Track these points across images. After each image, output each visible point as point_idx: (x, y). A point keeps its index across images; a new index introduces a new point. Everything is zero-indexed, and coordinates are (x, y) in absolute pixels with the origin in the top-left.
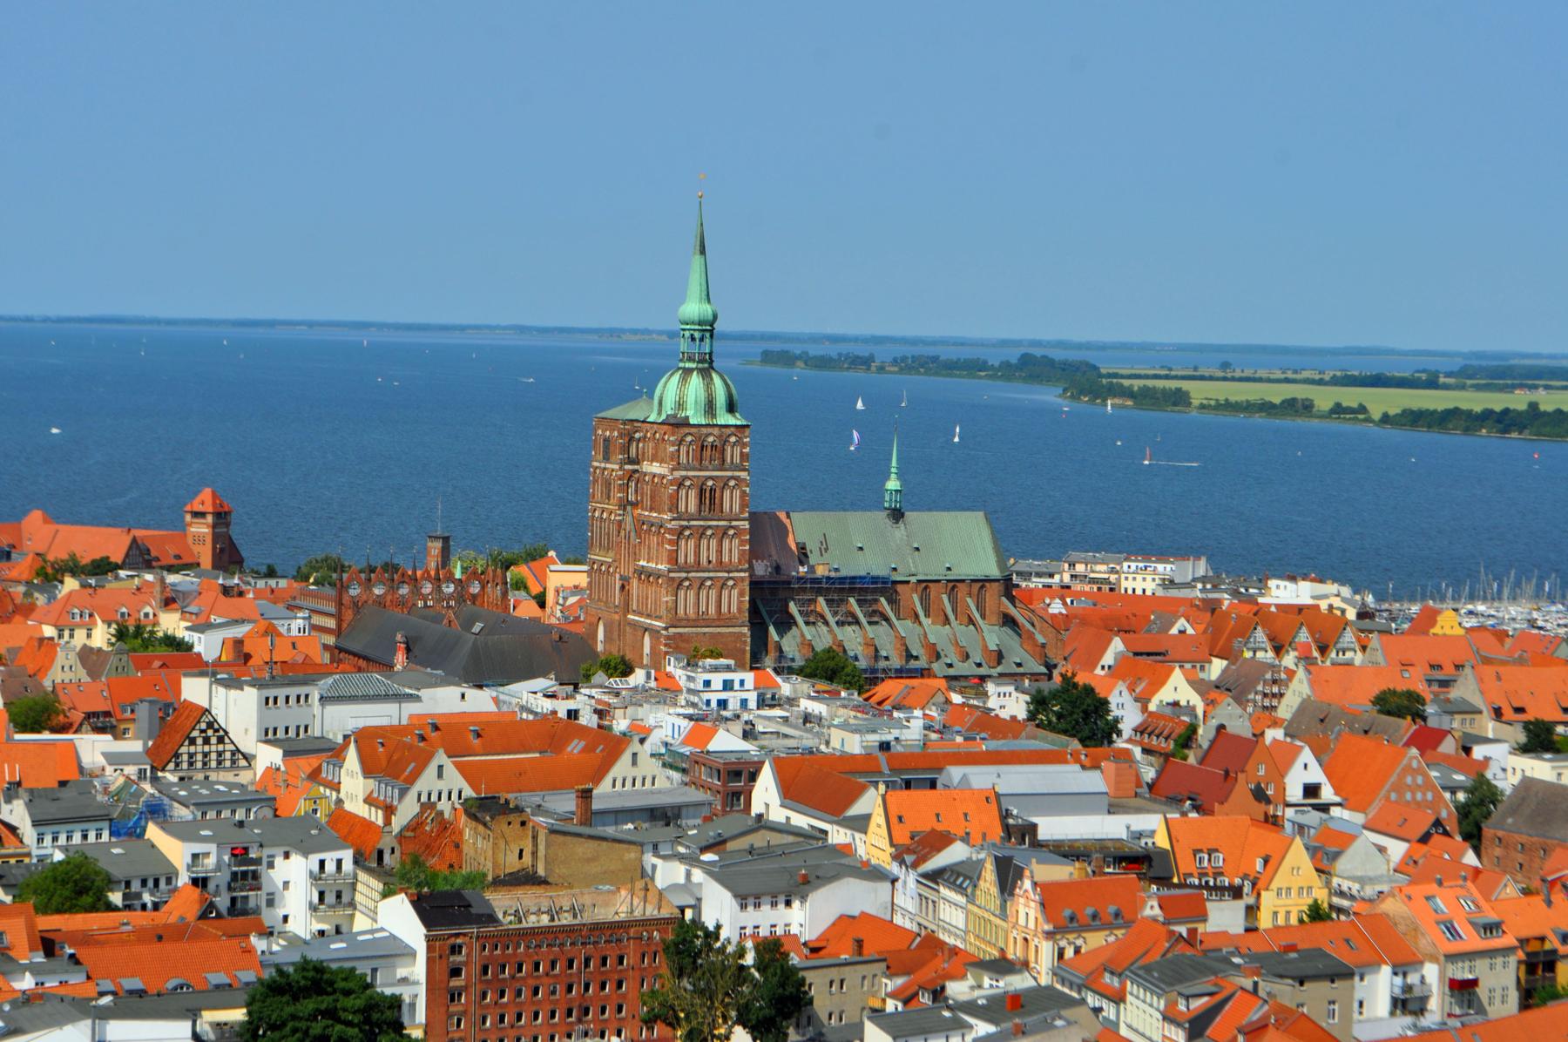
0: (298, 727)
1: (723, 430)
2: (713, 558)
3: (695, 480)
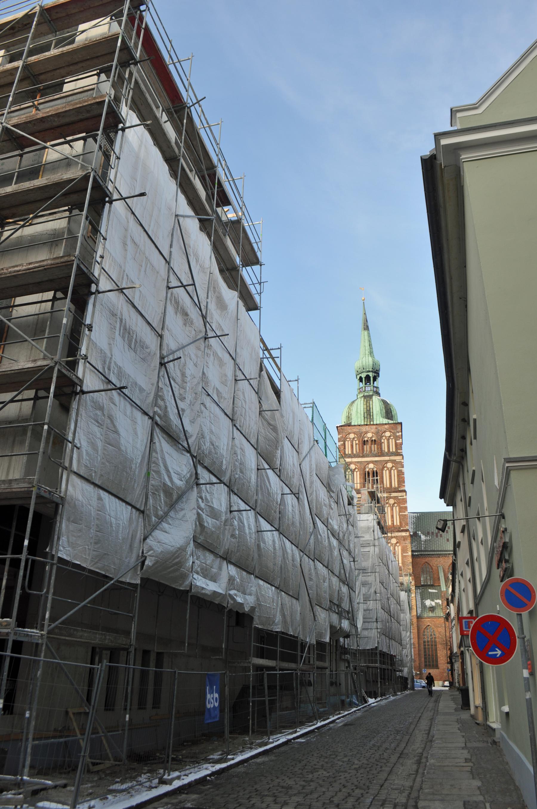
3: (359, 465)
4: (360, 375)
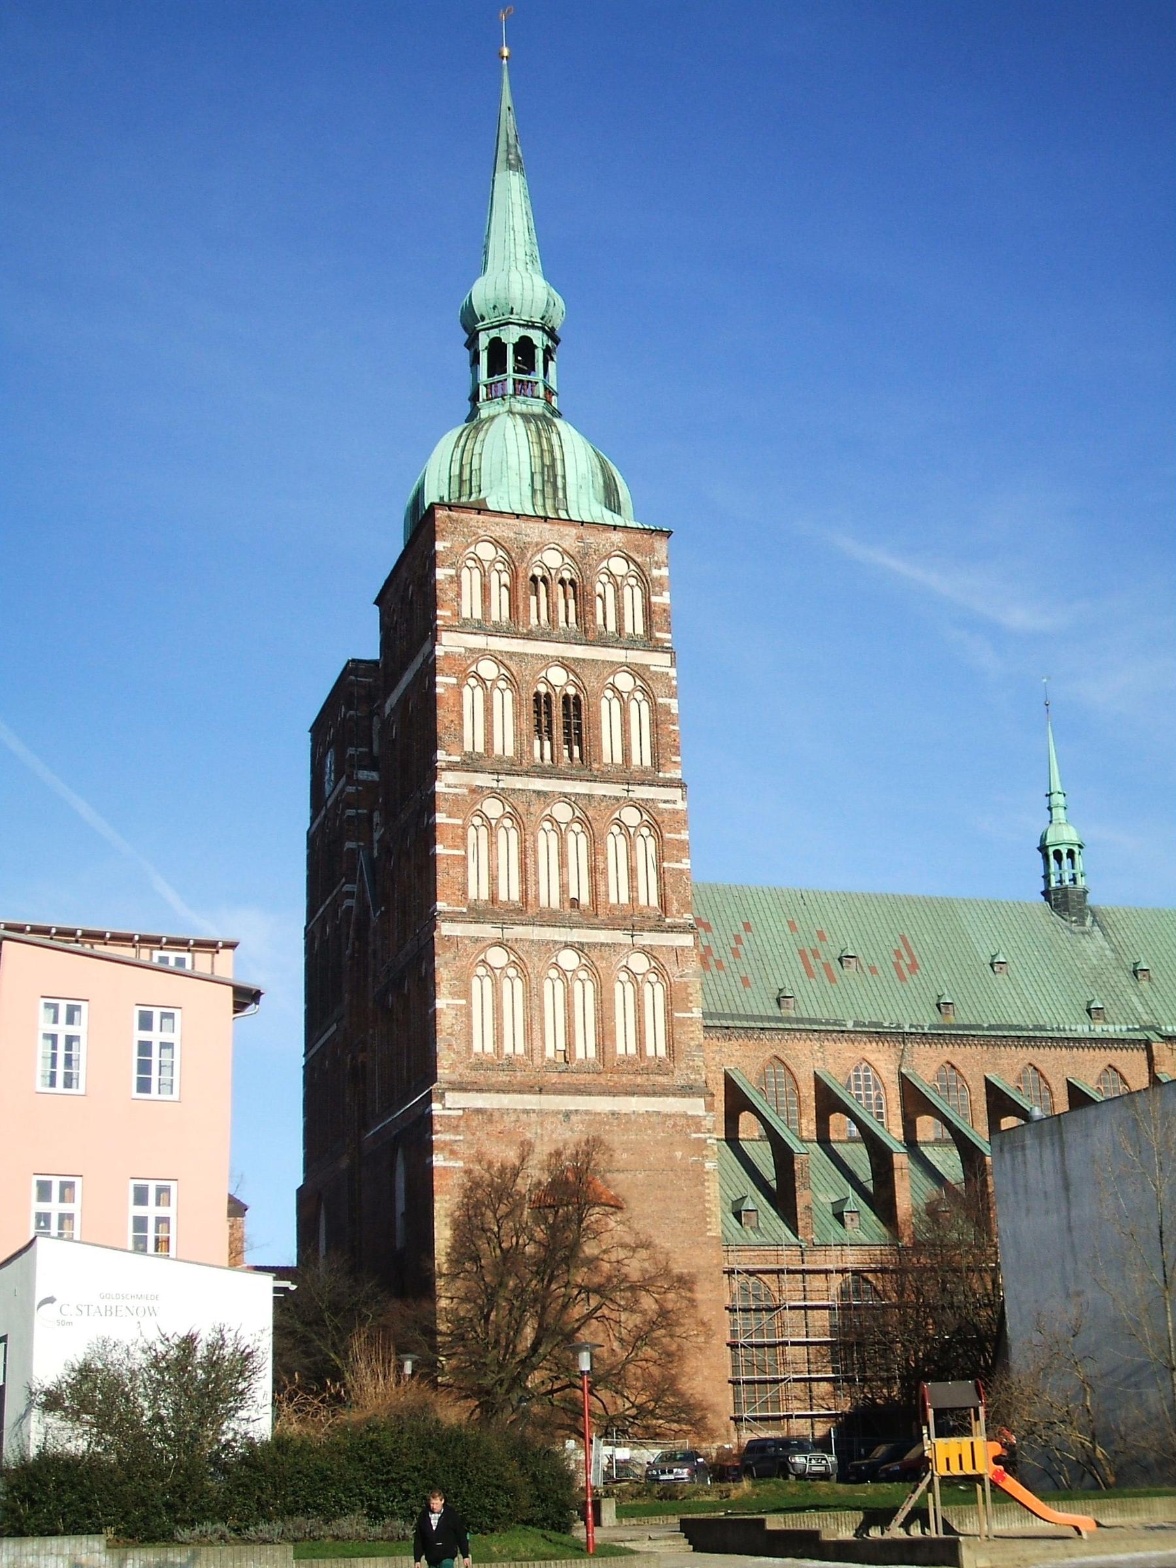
1: (594, 538)
2: (581, 890)
4: (494, 333)
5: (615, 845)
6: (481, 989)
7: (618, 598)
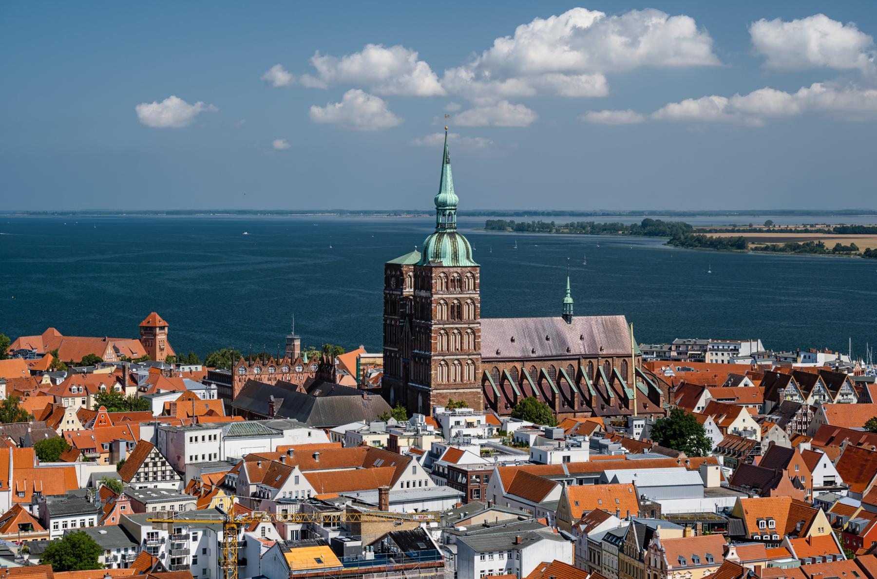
0: (210, 456)
1: (463, 269)
5: (466, 337)
6: (439, 369)
7: (468, 282)
